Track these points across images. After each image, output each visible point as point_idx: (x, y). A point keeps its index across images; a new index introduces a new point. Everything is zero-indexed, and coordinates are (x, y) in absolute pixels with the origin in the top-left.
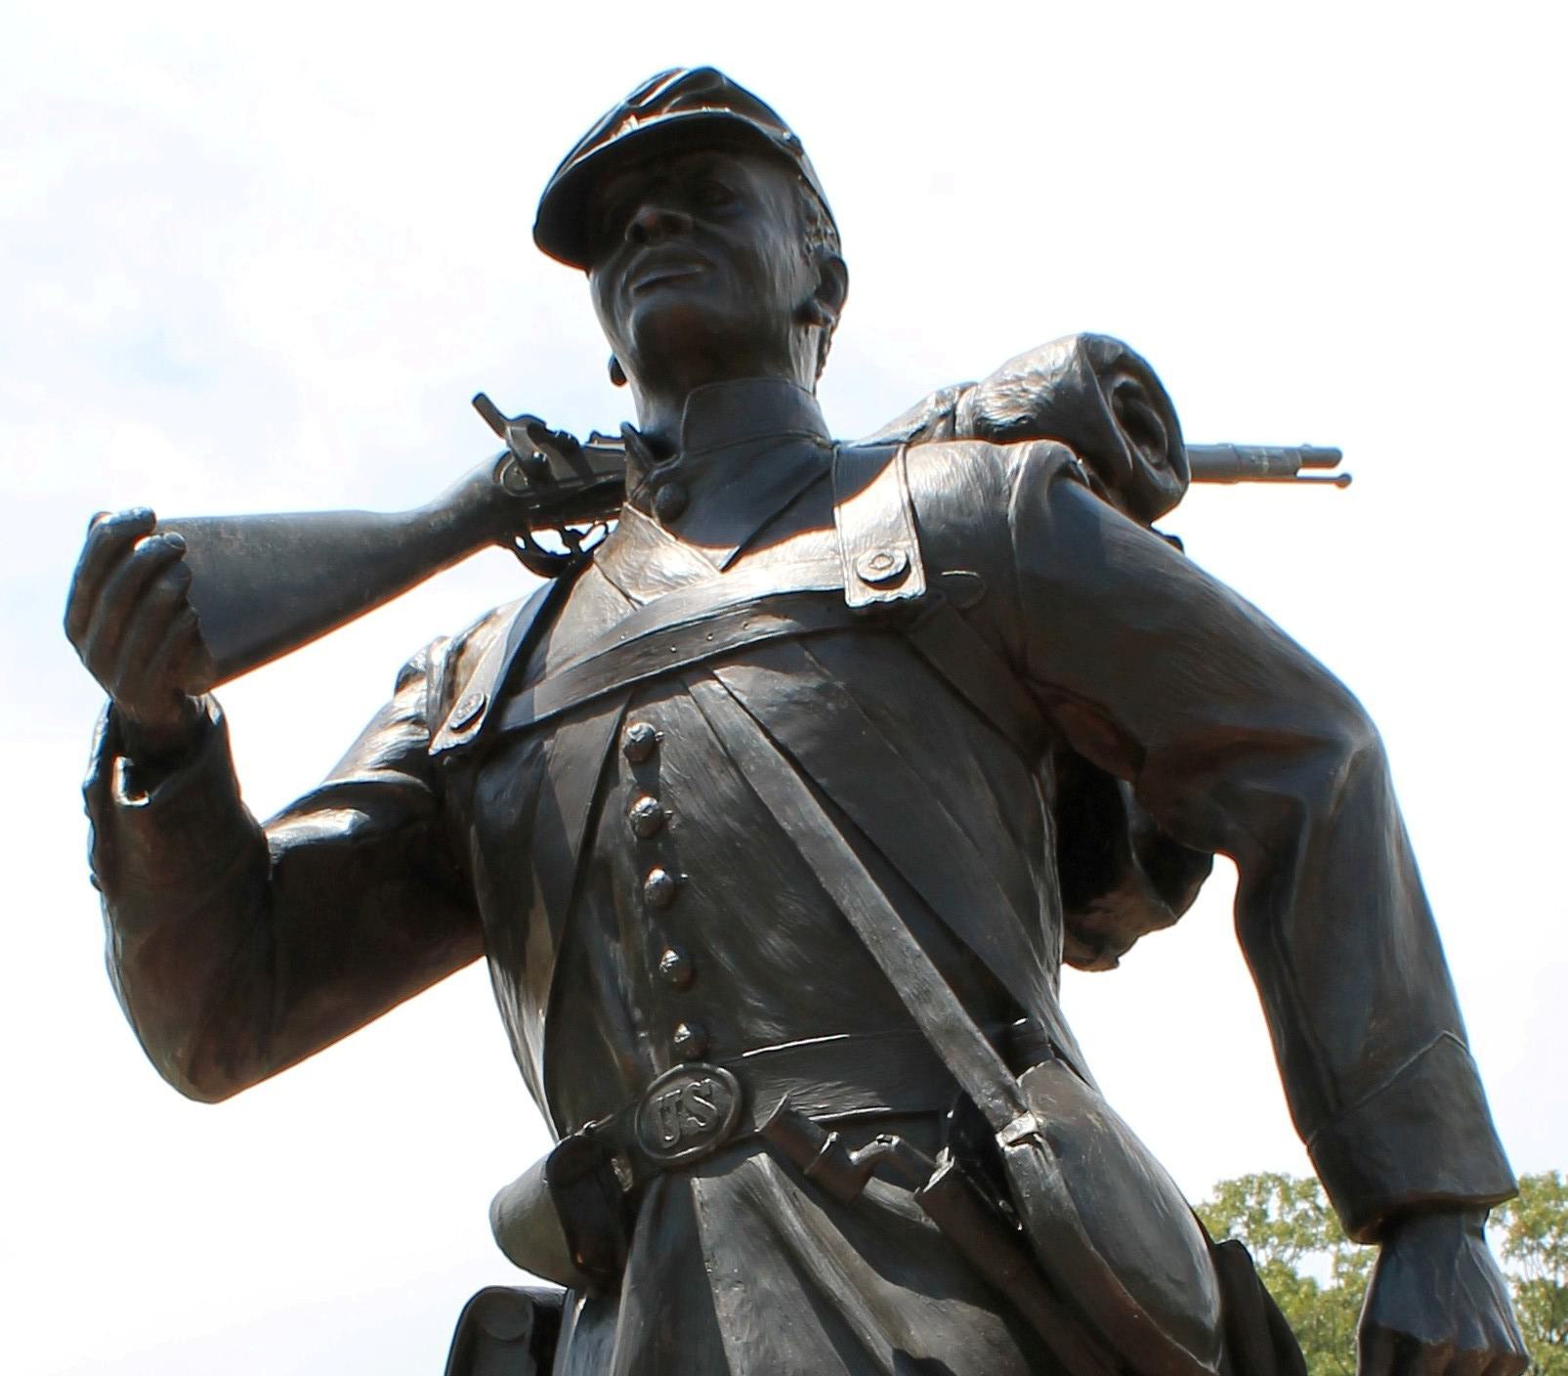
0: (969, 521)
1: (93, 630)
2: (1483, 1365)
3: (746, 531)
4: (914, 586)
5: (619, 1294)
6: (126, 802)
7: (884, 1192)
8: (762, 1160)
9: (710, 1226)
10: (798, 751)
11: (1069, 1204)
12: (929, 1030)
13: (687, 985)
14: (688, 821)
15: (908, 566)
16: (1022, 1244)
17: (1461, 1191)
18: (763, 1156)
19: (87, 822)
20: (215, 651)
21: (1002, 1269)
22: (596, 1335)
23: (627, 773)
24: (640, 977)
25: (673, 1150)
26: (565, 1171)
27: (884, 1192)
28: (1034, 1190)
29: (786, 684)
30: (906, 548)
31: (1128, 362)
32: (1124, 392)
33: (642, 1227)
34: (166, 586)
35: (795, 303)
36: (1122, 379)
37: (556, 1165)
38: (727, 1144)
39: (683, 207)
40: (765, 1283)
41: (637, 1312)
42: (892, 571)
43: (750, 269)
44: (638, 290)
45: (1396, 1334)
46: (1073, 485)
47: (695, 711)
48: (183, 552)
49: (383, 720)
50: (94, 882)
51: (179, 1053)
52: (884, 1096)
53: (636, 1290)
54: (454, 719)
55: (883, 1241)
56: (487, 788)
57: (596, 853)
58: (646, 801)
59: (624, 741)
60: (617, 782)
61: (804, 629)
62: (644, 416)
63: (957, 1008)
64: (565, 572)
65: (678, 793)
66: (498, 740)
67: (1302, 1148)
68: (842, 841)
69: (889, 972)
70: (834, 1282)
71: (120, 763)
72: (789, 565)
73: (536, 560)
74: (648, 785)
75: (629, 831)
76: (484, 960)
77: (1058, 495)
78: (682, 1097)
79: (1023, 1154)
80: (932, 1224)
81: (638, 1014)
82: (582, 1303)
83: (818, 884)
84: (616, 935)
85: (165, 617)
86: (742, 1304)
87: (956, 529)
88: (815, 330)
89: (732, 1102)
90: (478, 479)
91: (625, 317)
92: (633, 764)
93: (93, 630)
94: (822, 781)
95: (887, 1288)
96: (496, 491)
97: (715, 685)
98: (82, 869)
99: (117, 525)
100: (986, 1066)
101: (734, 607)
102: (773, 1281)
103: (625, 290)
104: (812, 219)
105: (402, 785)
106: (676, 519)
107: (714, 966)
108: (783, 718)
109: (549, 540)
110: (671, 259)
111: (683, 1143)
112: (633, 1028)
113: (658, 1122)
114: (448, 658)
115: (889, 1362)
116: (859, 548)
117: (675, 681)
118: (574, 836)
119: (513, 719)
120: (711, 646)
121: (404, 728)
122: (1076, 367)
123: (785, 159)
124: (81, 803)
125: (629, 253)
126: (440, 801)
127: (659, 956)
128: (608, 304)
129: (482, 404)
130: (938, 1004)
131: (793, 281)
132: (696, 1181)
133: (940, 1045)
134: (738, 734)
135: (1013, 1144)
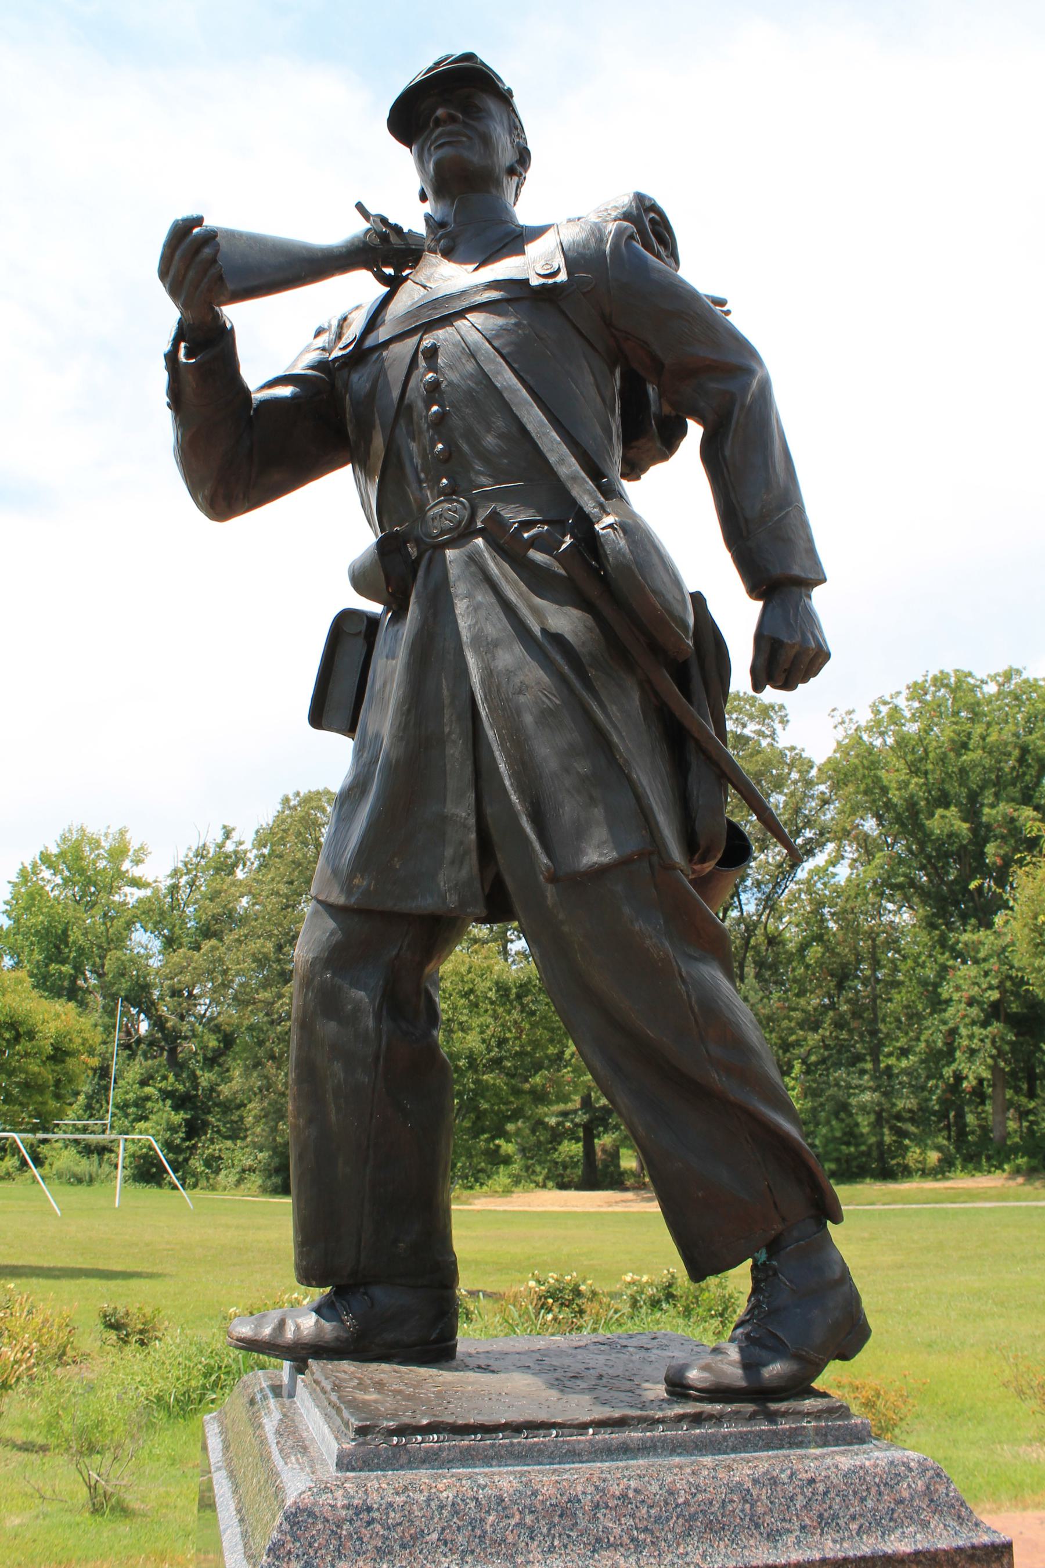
0: (587, 252)
1: (172, 273)
2: (812, 654)
3: (482, 258)
4: (563, 277)
5: (407, 610)
6: (184, 360)
7: (537, 556)
8: (480, 541)
9: (454, 571)
10: (504, 351)
11: (629, 556)
12: (563, 477)
13: (447, 460)
14: (450, 384)
15: (559, 268)
16: (605, 582)
17: (803, 575)
18: (480, 539)
19: (166, 374)
20: (230, 286)
21: (593, 591)
22: (396, 628)
23: (422, 363)
24: (424, 456)
25: (437, 537)
26: (387, 547)
27: (537, 556)
28: (613, 550)
29: (498, 321)
30: (559, 261)
31: (654, 208)
32: (652, 220)
33: (421, 573)
34: (207, 251)
35: (508, 164)
36: (652, 215)
37: (381, 545)
38: (463, 534)
39: (455, 115)
40: (479, 598)
41: (417, 612)
42: (552, 270)
43: (487, 141)
44: (436, 148)
45: (773, 639)
46: (635, 243)
47: (455, 333)
48: (216, 236)
49: (307, 350)
50: (169, 405)
51: (206, 492)
52: (539, 511)
53: (418, 602)
54: (341, 345)
55: (538, 580)
56: (355, 377)
57: (406, 401)
58: (431, 375)
59: (421, 348)
60: (417, 367)
61: (509, 297)
62: (436, 212)
63: (578, 468)
64: (394, 284)
65: (446, 371)
66: (361, 353)
67: (729, 555)
68: (524, 391)
69: (545, 451)
70: (512, 596)
71: (183, 345)
72: (506, 268)
73: (383, 279)
74: (433, 367)
75: (422, 389)
76: (350, 466)
77: (627, 244)
78: (443, 512)
79: (608, 534)
80: (562, 572)
81: (422, 476)
82: (390, 614)
83: (511, 409)
84: (414, 440)
85: (205, 269)
86: (468, 607)
87: (582, 256)
88: (515, 179)
89: (467, 514)
90: (357, 237)
91: (428, 162)
92: (425, 358)
93: (172, 273)
94: (515, 366)
95: (538, 601)
96: (365, 243)
97: (465, 322)
98: (163, 399)
99: (185, 220)
100: (590, 493)
101: (477, 286)
102: (484, 597)
103: (429, 149)
104: (516, 128)
105: (315, 376)
106: (448, 254)
107: (459, 449)
108: (497, 336)
109: (389, 271)
110: (450, 134)
111: (442, 533)
112: (420, 482)
113: (430, 524)
114: (339, 321)
115: (538, 633)
116: (537, 263)
117: (446, 320)
118: (396, 393)
119: (369, 342)
120: (465, 304)
121: (318, 352)
122: (634, 204)
123: (505, 98)
124: (163, 363)
125: (432, 131)
126: (333, 385)
127: (435, 446)
128: (421, 160)
129: (360, 207)
130: (567, 465)
131: (506, 156)
132: (447, 552)
133: (569, 485)
134: (476, 343)
135: (603, 529)
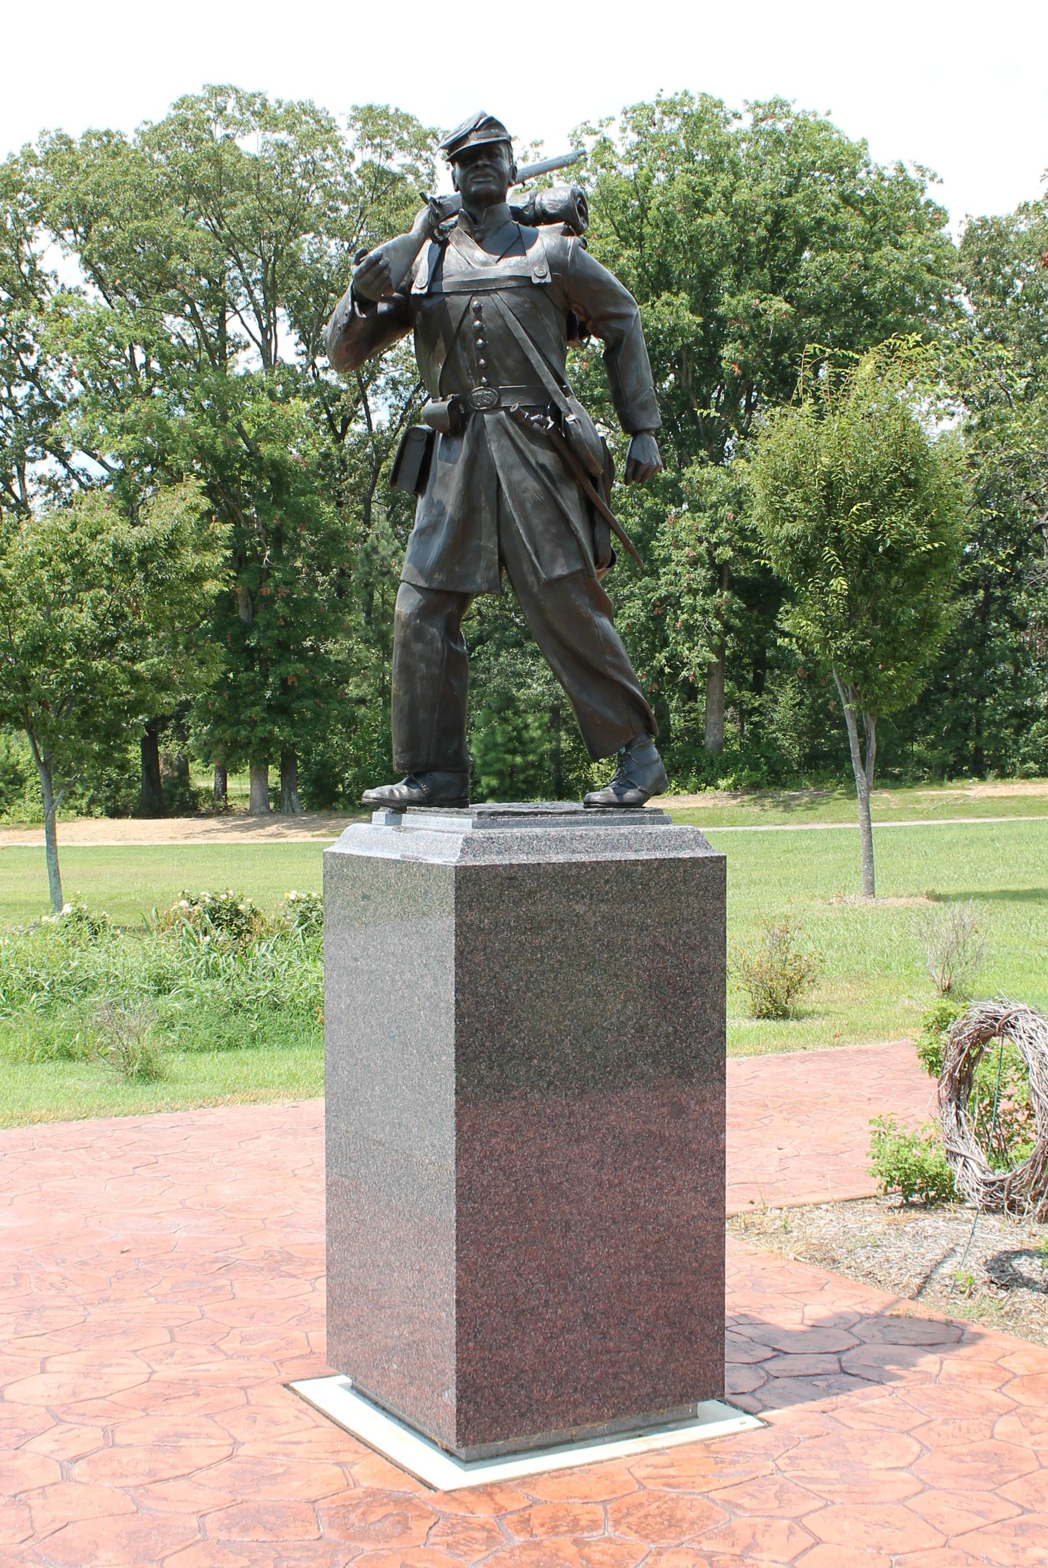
4: (548, 279)
8: (503, 413)
9: (489, 427)
16: (567, 441)
21: (561, 447)
30: (546, 269)
38: (495, 408)
55: (533, 435)
117: (486, 292)
